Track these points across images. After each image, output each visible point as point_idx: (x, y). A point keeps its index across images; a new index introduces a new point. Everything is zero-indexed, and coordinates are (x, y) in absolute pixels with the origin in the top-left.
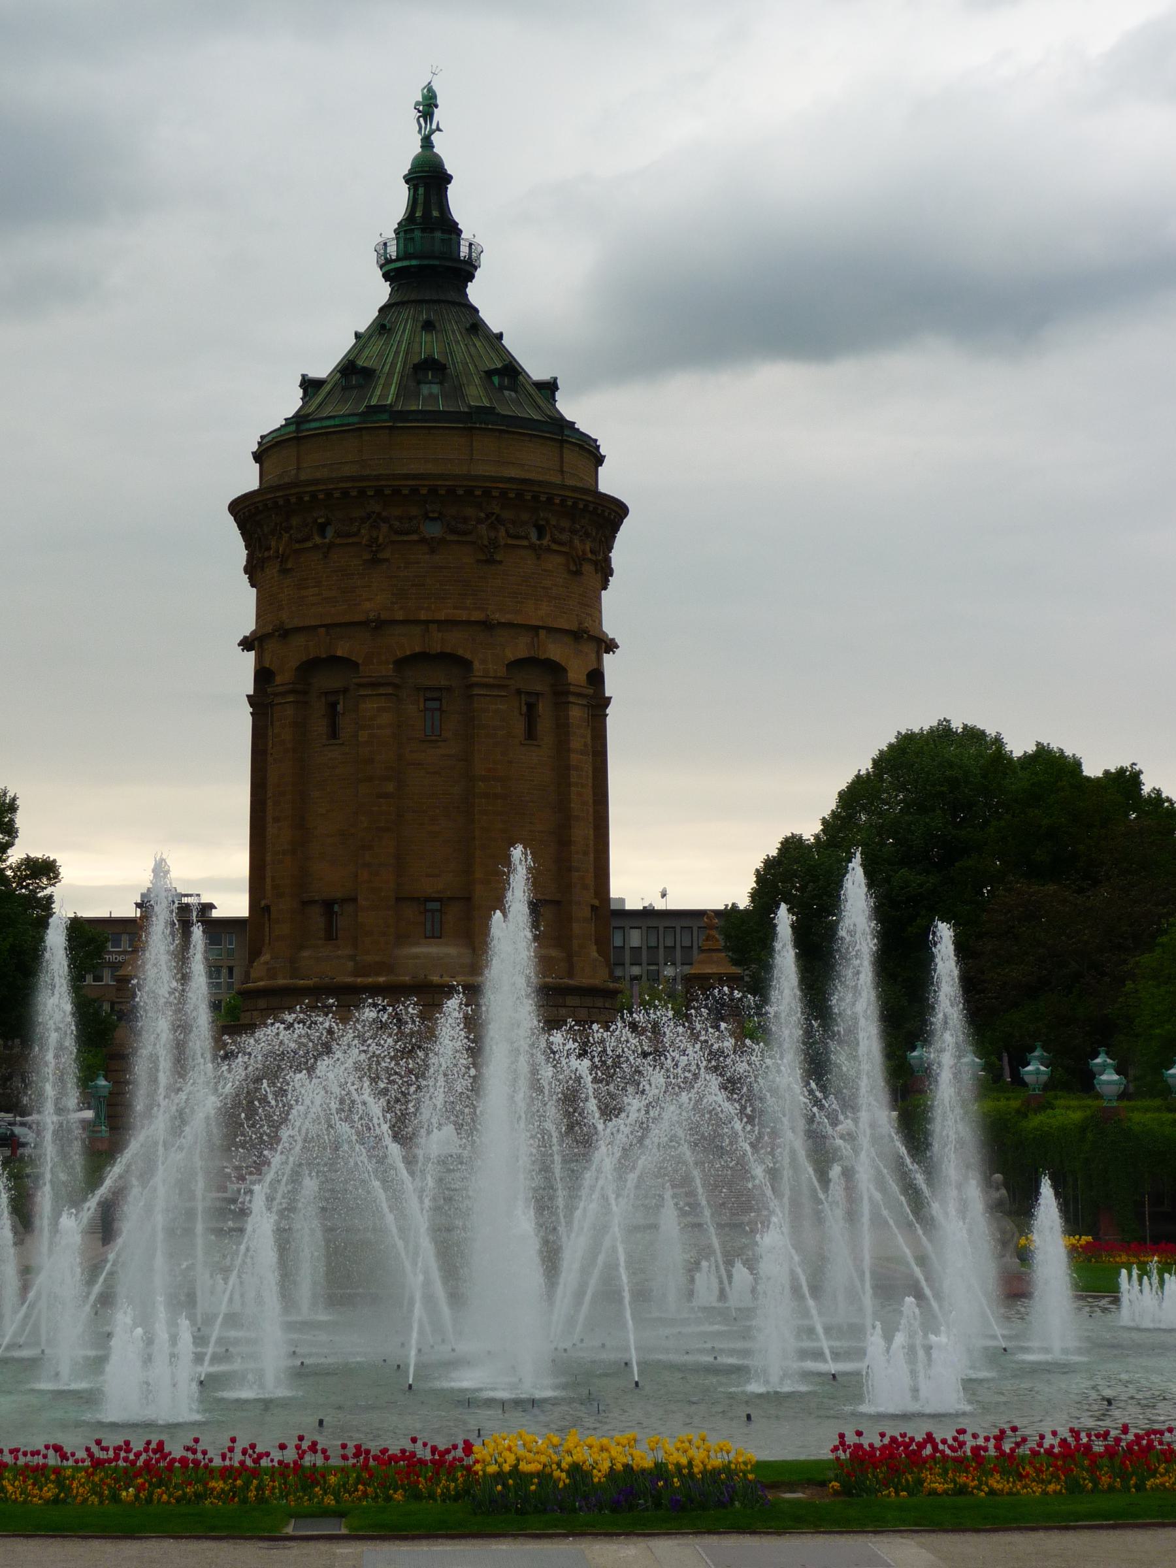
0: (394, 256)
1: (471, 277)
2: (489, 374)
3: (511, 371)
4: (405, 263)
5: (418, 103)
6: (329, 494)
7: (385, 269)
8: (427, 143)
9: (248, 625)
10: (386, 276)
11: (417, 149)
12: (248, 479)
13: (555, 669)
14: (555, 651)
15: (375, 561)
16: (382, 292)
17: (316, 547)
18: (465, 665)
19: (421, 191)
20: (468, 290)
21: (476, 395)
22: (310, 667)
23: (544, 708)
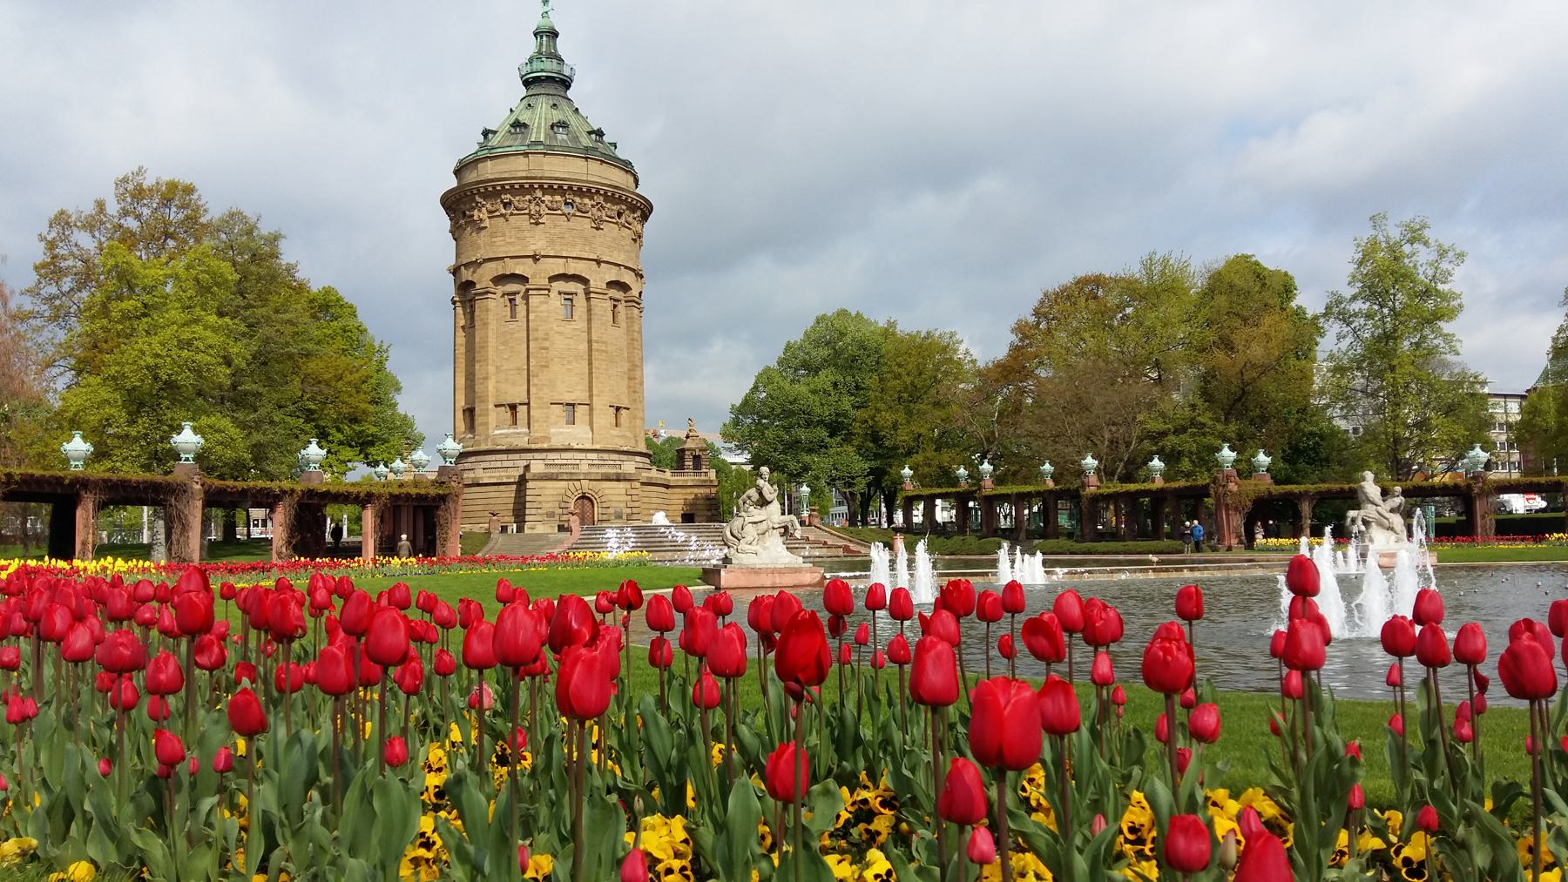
1: (568, 87)
2: (590, 133)
3: (600, 133)
6: (512, 186)
9: (452, 262)
10: (527, 83)
12: (454, 183)
13: (624, 287)
14: (628, 278)
15: (537, 224)
17: (502, 215)
18: (584, 281)
21: (586, 141)
22: (500, 279)
23: (621, 307)
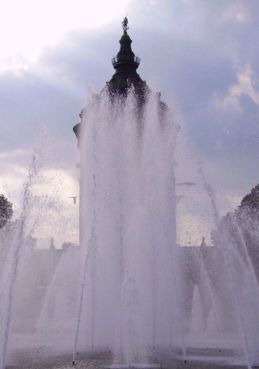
0: (117, 61)
1: (137, 67)
4: (120, 63)
5: (123, 22)
7: (114, 65)
8: (125, 32)
10: (115, 67)
11: (122, 34)
16: (114, 71)
19: (124, 44)
20: (136, 71)
